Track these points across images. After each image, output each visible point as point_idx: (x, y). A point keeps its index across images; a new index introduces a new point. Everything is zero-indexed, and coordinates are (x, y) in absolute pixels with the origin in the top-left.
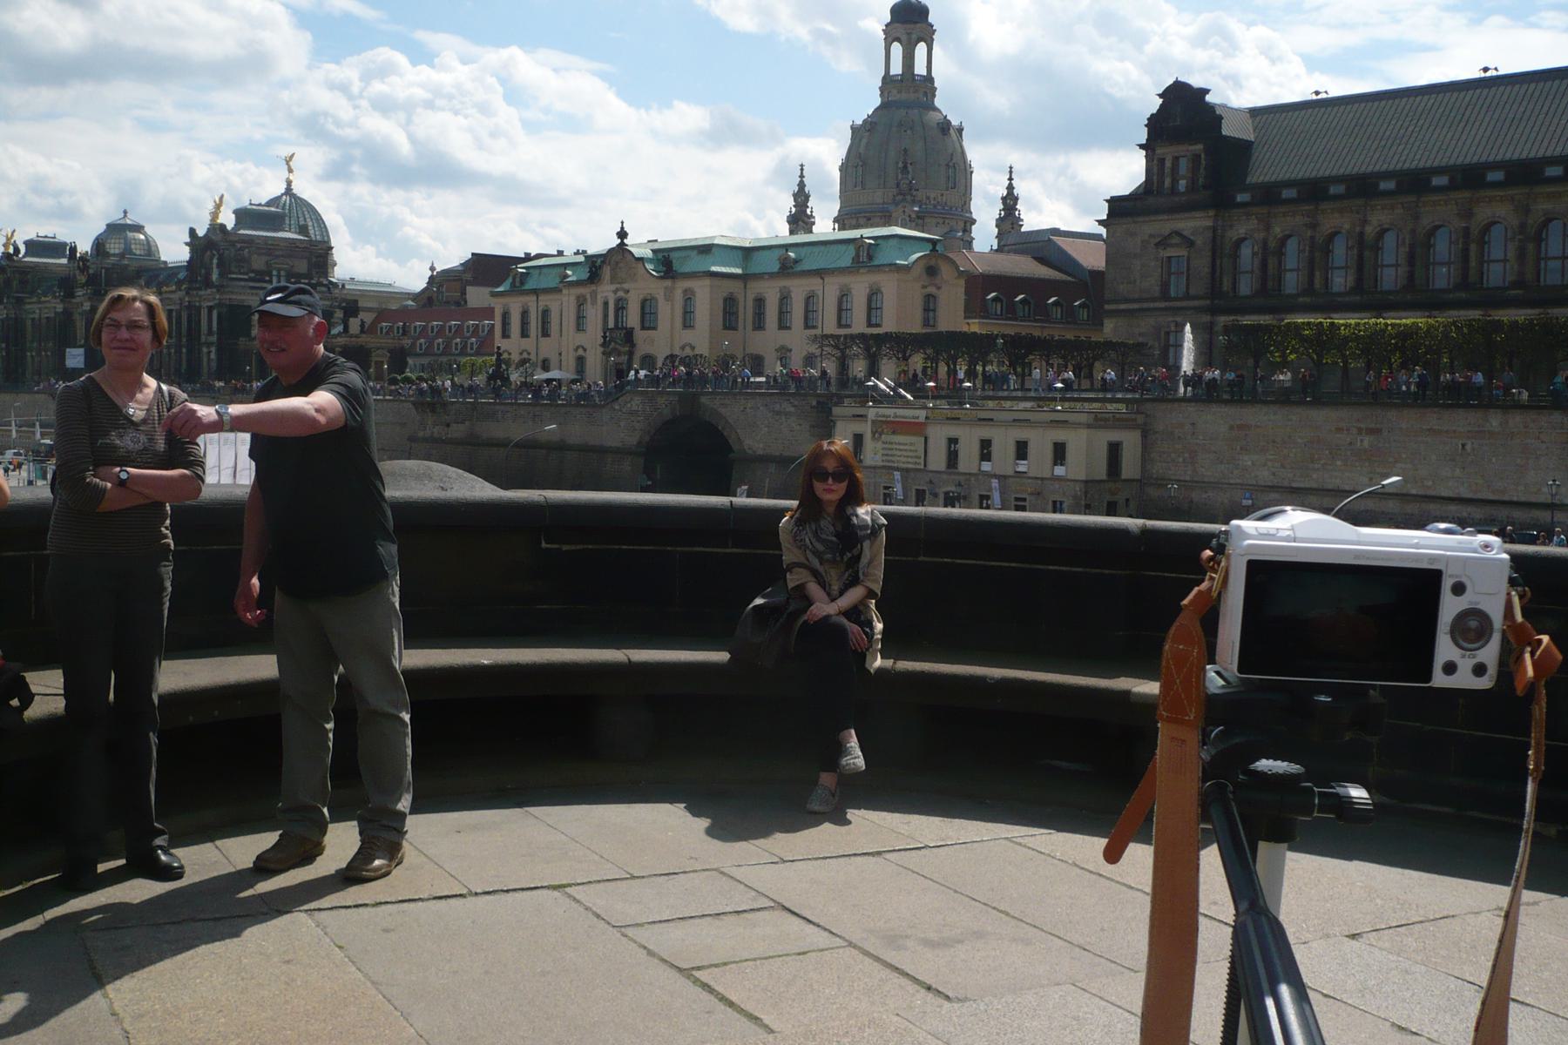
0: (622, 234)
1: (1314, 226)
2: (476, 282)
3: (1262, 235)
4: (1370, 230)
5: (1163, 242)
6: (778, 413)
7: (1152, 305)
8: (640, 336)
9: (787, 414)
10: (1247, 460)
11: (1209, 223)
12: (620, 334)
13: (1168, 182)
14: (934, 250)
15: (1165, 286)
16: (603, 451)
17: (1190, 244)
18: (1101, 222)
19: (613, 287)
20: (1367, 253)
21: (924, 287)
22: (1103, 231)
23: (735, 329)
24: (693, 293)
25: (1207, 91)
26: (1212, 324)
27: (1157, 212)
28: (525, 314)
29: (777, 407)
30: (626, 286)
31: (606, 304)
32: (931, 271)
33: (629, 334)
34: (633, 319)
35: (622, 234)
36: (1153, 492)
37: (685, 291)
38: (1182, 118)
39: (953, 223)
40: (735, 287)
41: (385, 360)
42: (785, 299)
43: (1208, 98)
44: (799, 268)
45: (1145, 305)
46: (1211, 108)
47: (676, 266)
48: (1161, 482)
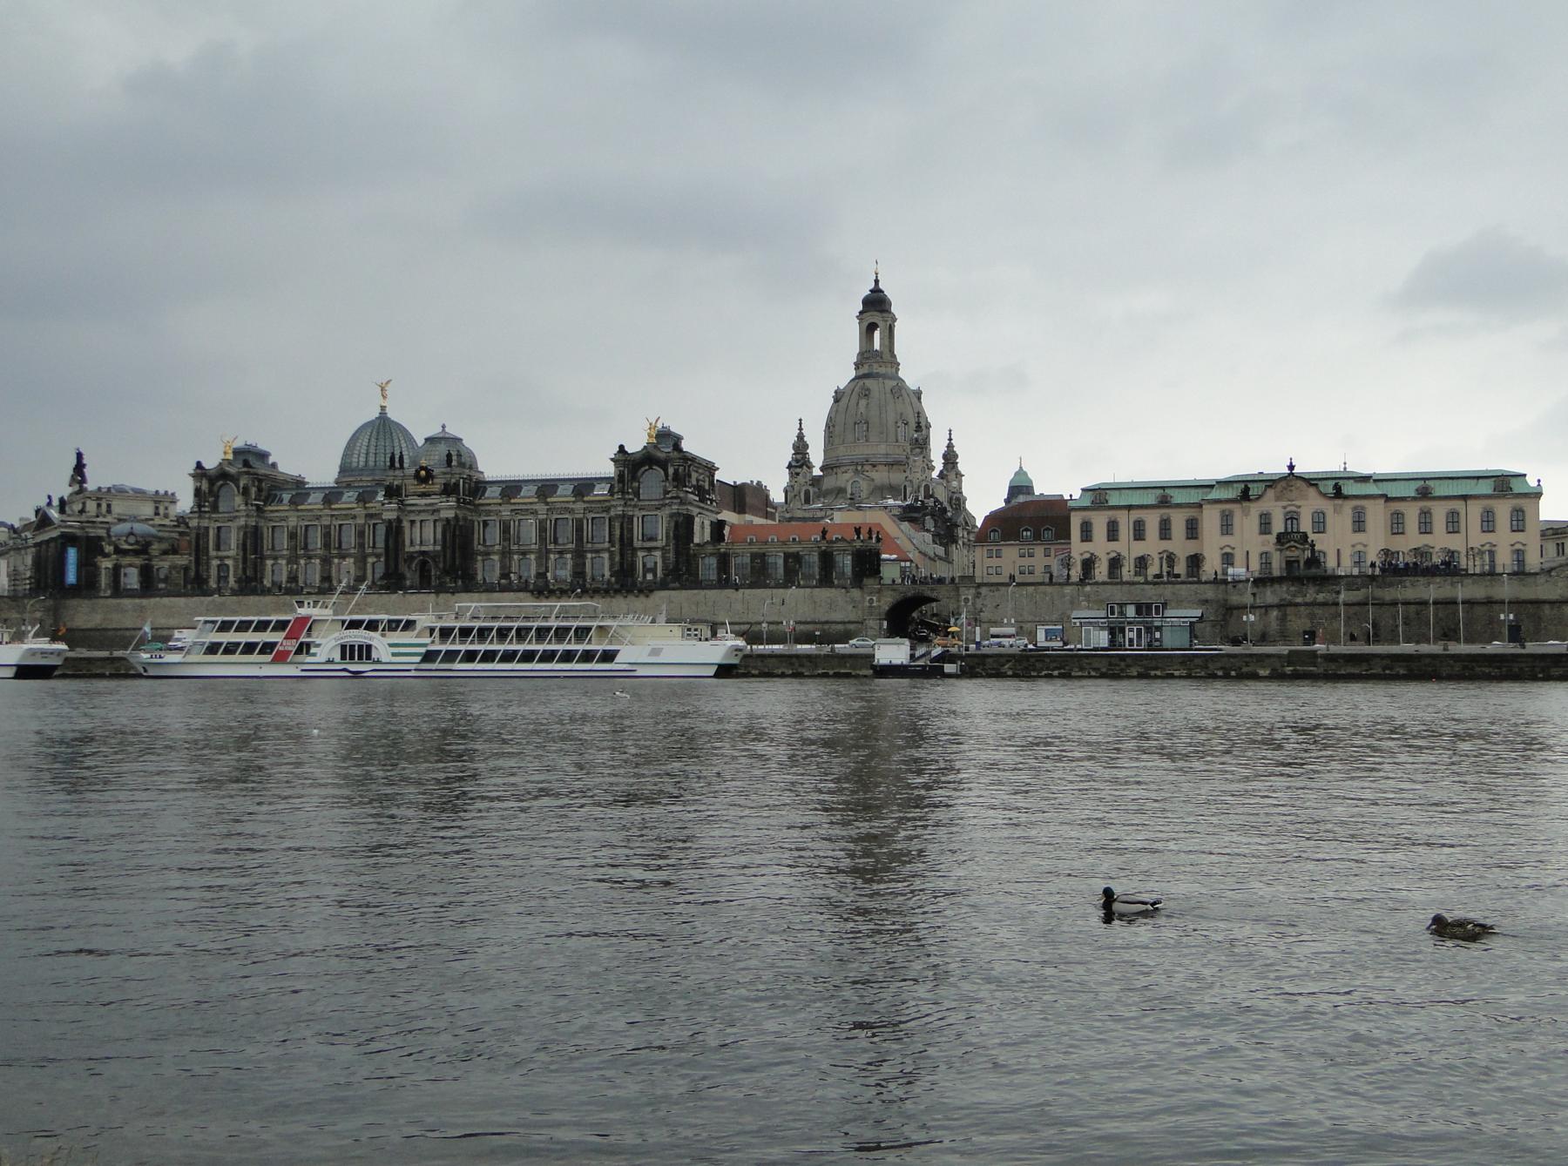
0: (1291, 467)
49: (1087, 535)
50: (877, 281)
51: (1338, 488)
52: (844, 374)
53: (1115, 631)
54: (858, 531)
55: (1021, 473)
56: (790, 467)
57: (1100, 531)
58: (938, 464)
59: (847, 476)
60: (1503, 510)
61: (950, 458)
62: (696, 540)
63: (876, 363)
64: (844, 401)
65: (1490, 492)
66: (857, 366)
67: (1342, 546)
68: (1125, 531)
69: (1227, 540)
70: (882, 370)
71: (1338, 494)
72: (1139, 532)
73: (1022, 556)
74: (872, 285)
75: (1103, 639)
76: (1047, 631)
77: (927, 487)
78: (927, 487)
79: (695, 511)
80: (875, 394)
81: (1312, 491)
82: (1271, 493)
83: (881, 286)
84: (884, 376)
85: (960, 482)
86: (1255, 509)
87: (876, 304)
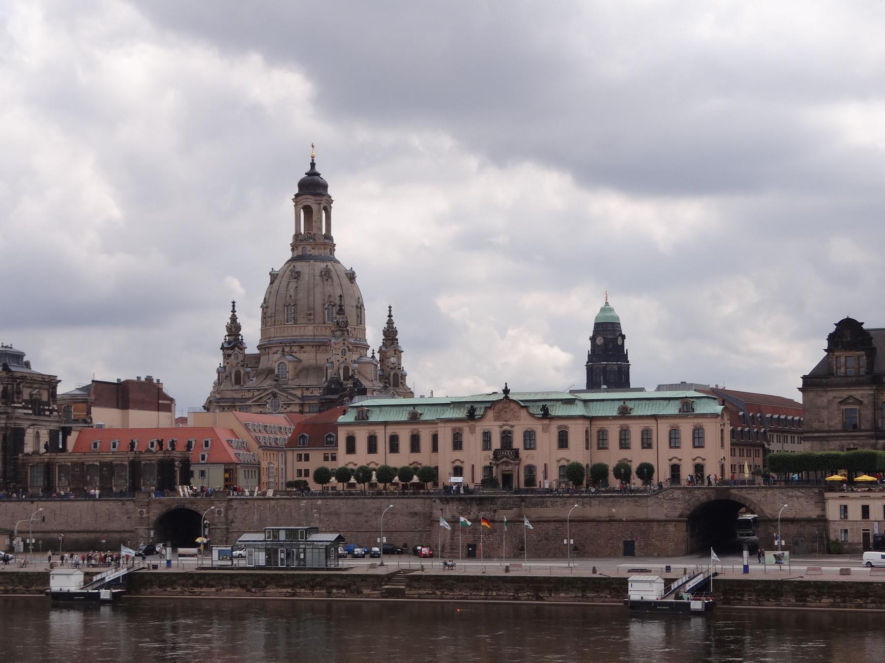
0: (506, 391)
5: (844, 402)
7: (837, 434)
8: (523, 453)
9: (801, 497)
11: (872, 392)
17: (860, 403)
19: (501, 423)
29: (790, 494)
30: (511, 423)
31: (487, 436)
33: (516, 452)
35: (506, 391)
39: (361, 351)
40: (587, 423)
44: (634, 413)
45: (833, 434)
46: (866, 333)
49: (351, 448)
50: (313, 165)
51: (545, 409)
52: (280, 254)
53: (271, 554)
54: (160, 443)
55: (606, 308)
56: (222, 348)
57: (361, 444)
58: (374, 338)
59: (278, 356)
60: (686, 428)
61: (390, 334)
62: (28, 449)
64: (277, 282)
65: (676, 412)
66: (294, 247)
67: (546, 459)
68: (382, 444)
69: (458, 455)
70: (315, 252)
71: (546, 415)
72: (394, 447)
73: (326, 459)
74: (308, 168)
75: (261, 558)
76: (219, 551)
77: (346, 369)
78: (346, 369)
79: (25, 424)
80: (305, 278)
81: (523, 412)
82: (491, 414)
83: (318, 169)
84: (316, 259)
85: (399, 358)
86: (481, 427)
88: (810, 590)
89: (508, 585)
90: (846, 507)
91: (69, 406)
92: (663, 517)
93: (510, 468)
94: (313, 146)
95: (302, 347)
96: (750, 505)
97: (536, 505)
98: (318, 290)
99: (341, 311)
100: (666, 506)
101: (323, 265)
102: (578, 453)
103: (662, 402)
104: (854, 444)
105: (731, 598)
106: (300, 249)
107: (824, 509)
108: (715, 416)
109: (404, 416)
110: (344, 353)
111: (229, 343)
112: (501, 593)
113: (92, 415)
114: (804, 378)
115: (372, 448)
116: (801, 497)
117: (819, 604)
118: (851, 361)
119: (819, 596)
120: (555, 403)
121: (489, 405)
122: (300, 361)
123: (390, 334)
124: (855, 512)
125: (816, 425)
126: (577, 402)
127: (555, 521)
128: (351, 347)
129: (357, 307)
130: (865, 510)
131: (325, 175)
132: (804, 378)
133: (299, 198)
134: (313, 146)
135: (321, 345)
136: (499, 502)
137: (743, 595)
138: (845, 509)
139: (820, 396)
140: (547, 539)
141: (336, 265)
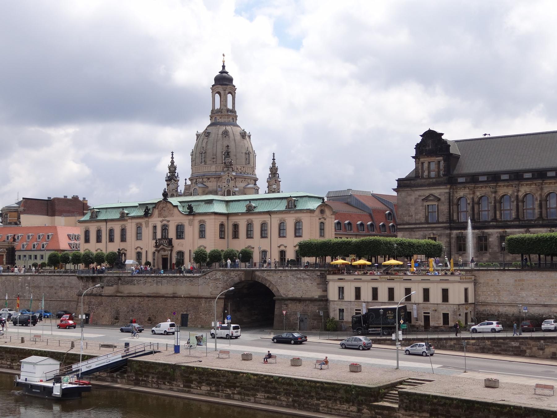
1: (495, 192)
2: (25, 212)
3: (471, 196)
4: (521, 194)
5: (426, 199)
6: (300, 278)
7: (421, 226)
8: (175, 242)
9: (306, 279)
10: (524, 294)
11: (447, 191)
12: (165, 242)
13: (426, 173)
14: (323, 202)
15: (427, 218)
16: (199, 298)
17: (439, 200)
18: (394, 190)
19: (161, 219)
20: (520, 204)
21: (320, 219)
22: (395, 194)
23: (224, 238)
24: (204, 221)
25: (442, 134)
26: (450, 234)
27: (422, 185)
28: (99, 232)
29: (299, 276)
30: (167, 219)
31: (155, 227)
32: (322, 212)
33: (170, 242)
34: (172, 234)
36: (481, 309)
37: (200, 221)
38: (431, 144)
39: (249, 181)
40: (223, 219)
41: (5, 254)
42: (250, 226)
43: (443, 137)
44: (256, 210)
45: (418, 226)
46: (445, 142)
47: (194, 210)
48: (485, 304)
50: (224, 67)
51: (190, 208)
61: (274, 171)
63: (224, 116)
65: (284, 208)
66: (211, 117)
69: (139, 243)
70: (222, 120)
74: (221, 69)
80: (212, 136)
82: (156, 212)
83: (227, 69)
84: (221, 124)
87: (223, 82)
88: (194, 377)
89: (8, 355)
90: (343, 288)
91: (7, 214)
92: (208, 295)
93: (166, 253)
94: (224, 55)
95: (209, 179)
96: (269, 285)
97: (128, 283)
98: (219, 143)
99: (228, 154)
100: (211, 285)
101: (223, 128)
102: (211, 244)
103: (277, 201)
104: (434, 234)
105: (141, 378)
106: (214, 119)
107: (326, 290)
108: (311, 211)
109: (117, 216)
110: (228, 181)
111: (169, 177)
112: (3, 362)
113: (21, 220)
114: (399, 181)
115: (99, 240)
116: (306, 279)
117: (200, 392)
118: (434, 164)
119: (200, 383)
120: (200, 203)
121: (154, 206)
122: (207, 187)
123: (274, 171)
124: (350, 295)
125: (406, 219)
126: (214, 202)
127: (139, 296)
128: (233, 178)
129: (246, 153)
130: (358, 291)
131: (232, 72)
132: (399, 181)
133: (214, 87)
134: (224, 55)
135: (219, 177)
136: (105, 280)
137: (148, 377)
138: (341, 290)
139: (410, 195)
140: (133, 311)
141: (235, 128)
